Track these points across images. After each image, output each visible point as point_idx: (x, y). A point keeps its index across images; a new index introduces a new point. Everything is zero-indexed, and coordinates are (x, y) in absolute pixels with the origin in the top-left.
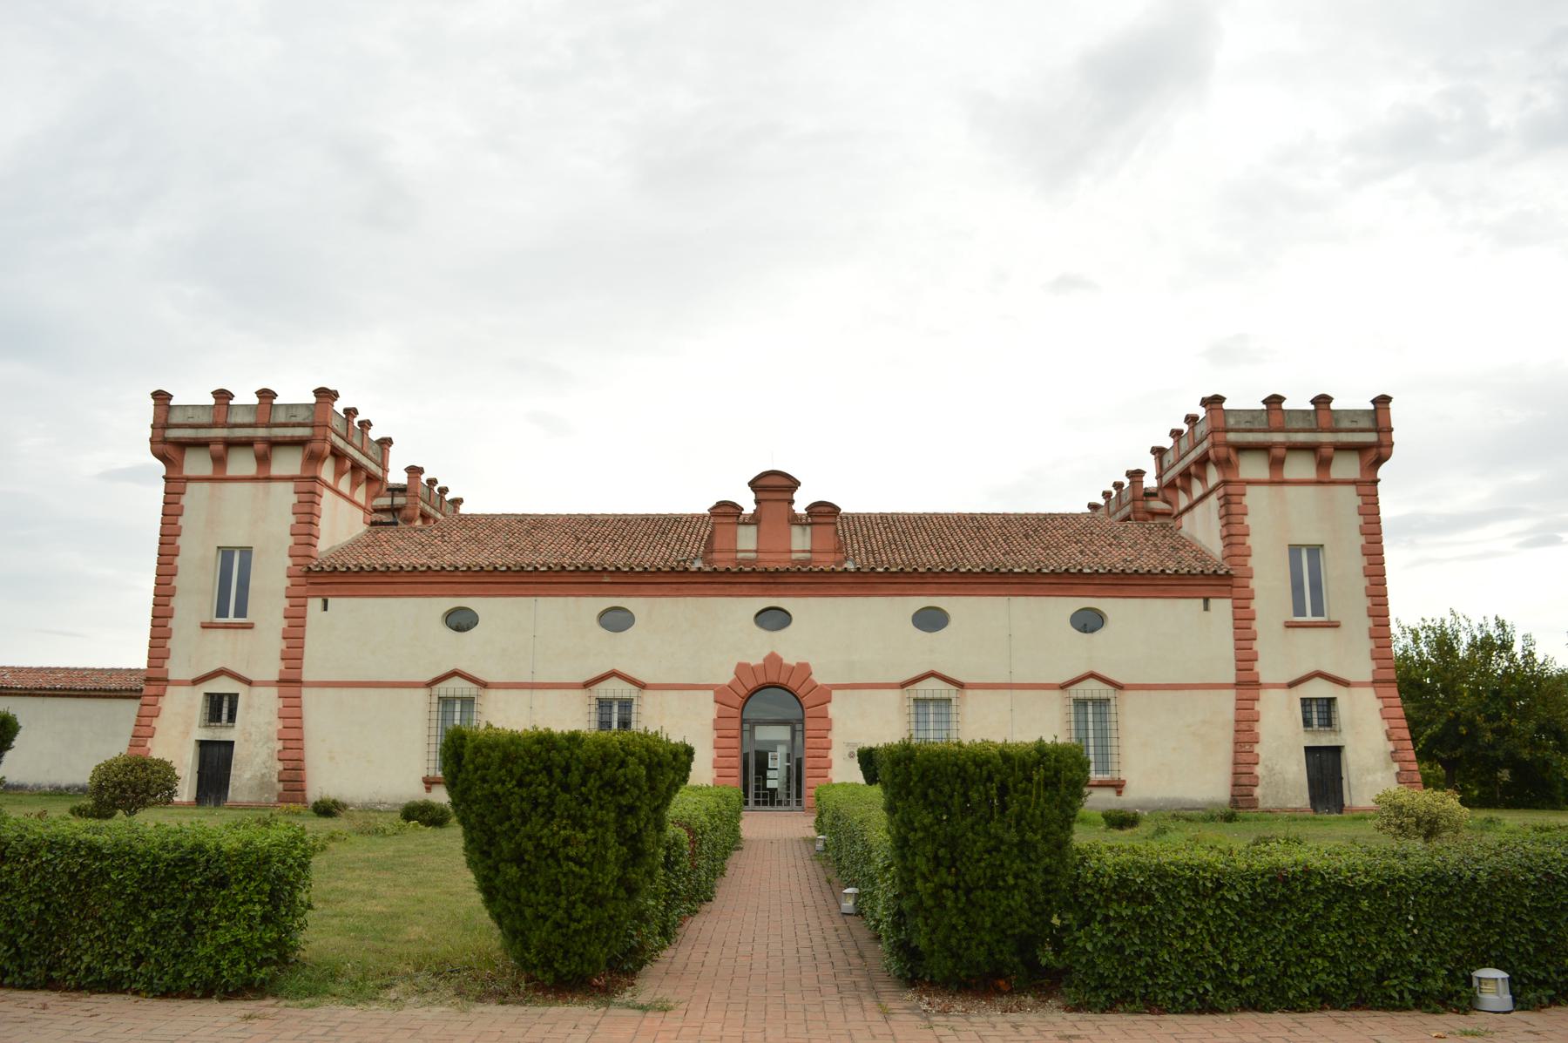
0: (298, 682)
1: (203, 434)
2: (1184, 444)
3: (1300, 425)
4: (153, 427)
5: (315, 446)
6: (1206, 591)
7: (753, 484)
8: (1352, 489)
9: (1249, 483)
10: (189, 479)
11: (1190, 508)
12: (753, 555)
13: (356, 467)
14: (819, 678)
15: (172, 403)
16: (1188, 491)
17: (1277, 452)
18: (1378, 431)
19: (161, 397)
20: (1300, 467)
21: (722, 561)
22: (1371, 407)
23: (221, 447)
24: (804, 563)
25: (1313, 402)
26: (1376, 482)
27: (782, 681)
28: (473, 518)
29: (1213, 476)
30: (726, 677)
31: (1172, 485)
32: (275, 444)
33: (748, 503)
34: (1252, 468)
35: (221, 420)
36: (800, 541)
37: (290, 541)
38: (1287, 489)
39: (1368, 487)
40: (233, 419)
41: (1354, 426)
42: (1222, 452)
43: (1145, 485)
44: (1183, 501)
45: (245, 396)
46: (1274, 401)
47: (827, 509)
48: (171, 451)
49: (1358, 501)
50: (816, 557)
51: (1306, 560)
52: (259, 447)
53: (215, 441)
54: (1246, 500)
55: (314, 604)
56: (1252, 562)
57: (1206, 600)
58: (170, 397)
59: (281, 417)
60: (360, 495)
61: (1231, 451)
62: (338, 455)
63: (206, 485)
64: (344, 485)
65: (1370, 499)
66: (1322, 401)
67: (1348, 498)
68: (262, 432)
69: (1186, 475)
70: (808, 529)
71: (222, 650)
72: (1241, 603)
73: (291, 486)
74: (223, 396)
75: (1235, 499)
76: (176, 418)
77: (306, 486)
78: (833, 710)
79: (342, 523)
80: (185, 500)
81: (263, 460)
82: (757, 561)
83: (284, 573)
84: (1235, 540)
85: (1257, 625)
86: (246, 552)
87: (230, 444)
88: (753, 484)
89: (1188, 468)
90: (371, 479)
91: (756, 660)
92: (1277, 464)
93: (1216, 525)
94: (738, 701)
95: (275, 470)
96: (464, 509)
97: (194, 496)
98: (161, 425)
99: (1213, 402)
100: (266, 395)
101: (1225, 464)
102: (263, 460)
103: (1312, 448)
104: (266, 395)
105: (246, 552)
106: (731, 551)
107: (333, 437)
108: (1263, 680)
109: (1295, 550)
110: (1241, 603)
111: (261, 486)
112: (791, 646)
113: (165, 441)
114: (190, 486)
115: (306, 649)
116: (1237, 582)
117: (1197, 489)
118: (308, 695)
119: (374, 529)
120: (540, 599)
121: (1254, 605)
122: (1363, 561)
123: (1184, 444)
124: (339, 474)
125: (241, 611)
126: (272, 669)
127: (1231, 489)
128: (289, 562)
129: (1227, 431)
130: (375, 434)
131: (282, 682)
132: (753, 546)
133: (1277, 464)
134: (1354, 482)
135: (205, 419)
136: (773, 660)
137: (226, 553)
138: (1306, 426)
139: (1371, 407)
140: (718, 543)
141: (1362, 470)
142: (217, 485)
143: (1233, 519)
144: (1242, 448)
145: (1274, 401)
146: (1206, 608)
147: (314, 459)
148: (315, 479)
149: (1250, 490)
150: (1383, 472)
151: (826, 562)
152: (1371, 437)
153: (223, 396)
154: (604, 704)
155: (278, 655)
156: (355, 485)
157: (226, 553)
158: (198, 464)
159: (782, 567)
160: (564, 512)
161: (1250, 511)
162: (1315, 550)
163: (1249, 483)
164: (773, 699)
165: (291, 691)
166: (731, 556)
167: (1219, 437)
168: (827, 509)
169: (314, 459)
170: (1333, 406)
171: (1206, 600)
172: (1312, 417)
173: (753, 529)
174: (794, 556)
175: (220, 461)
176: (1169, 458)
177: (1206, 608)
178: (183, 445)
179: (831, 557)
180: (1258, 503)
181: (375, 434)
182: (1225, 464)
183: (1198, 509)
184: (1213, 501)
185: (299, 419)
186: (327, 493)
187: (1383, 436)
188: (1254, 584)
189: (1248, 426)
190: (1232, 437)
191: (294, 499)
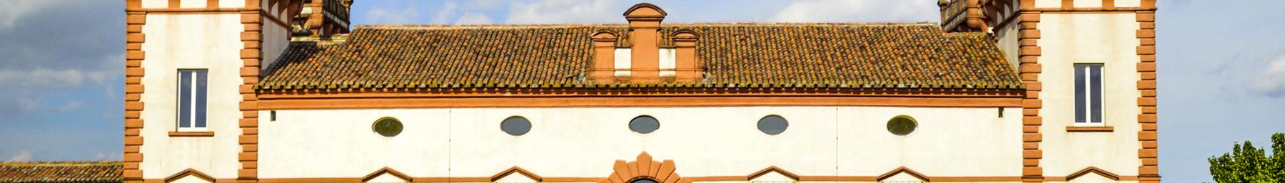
6: (1001, 102)
10: (147, 12)
21: (602, 78)
24: (668, 79)
27: (652, 174)
36: (667, 61)
38: (1075, 16)
49: (1138, 26)
50: (680, 74)
55: (264, 116)
57: (1001, 109)
63: (164, 16)
70: (673, 51)
71: (187, 153)
72: (1030, 111)
73: (238, 16)
75: (1030, 25)
82: (630, 78)
83: (237, 90)
86: (202, 73)
91: (631, 158)
105: (202, 73)
106: (609, 70)
108: (1044, 175)
109: (1079, 67)
110: (1030, 111)
111: (212, 16)
112: (657, 147)
115: (259, 152)
120: (453, 110)
121: (1041, 113)
125: (201, 121)
128: (241, 81)
136: (644, 158)
137: (185, 74)
143: (1026, 42)
146: (1001, 115)
149: (1042, 15)
151: (689, 78)
155: (237, 159)
156: (280, 11)
157: (185, 74)
159: (652, 83)
162: (1096, 68)
166: (610, 74)
171: (1001, 109)
174: (662, 74)
177: (1001, 115)
188: (1041, 95)
191: (242, 28)
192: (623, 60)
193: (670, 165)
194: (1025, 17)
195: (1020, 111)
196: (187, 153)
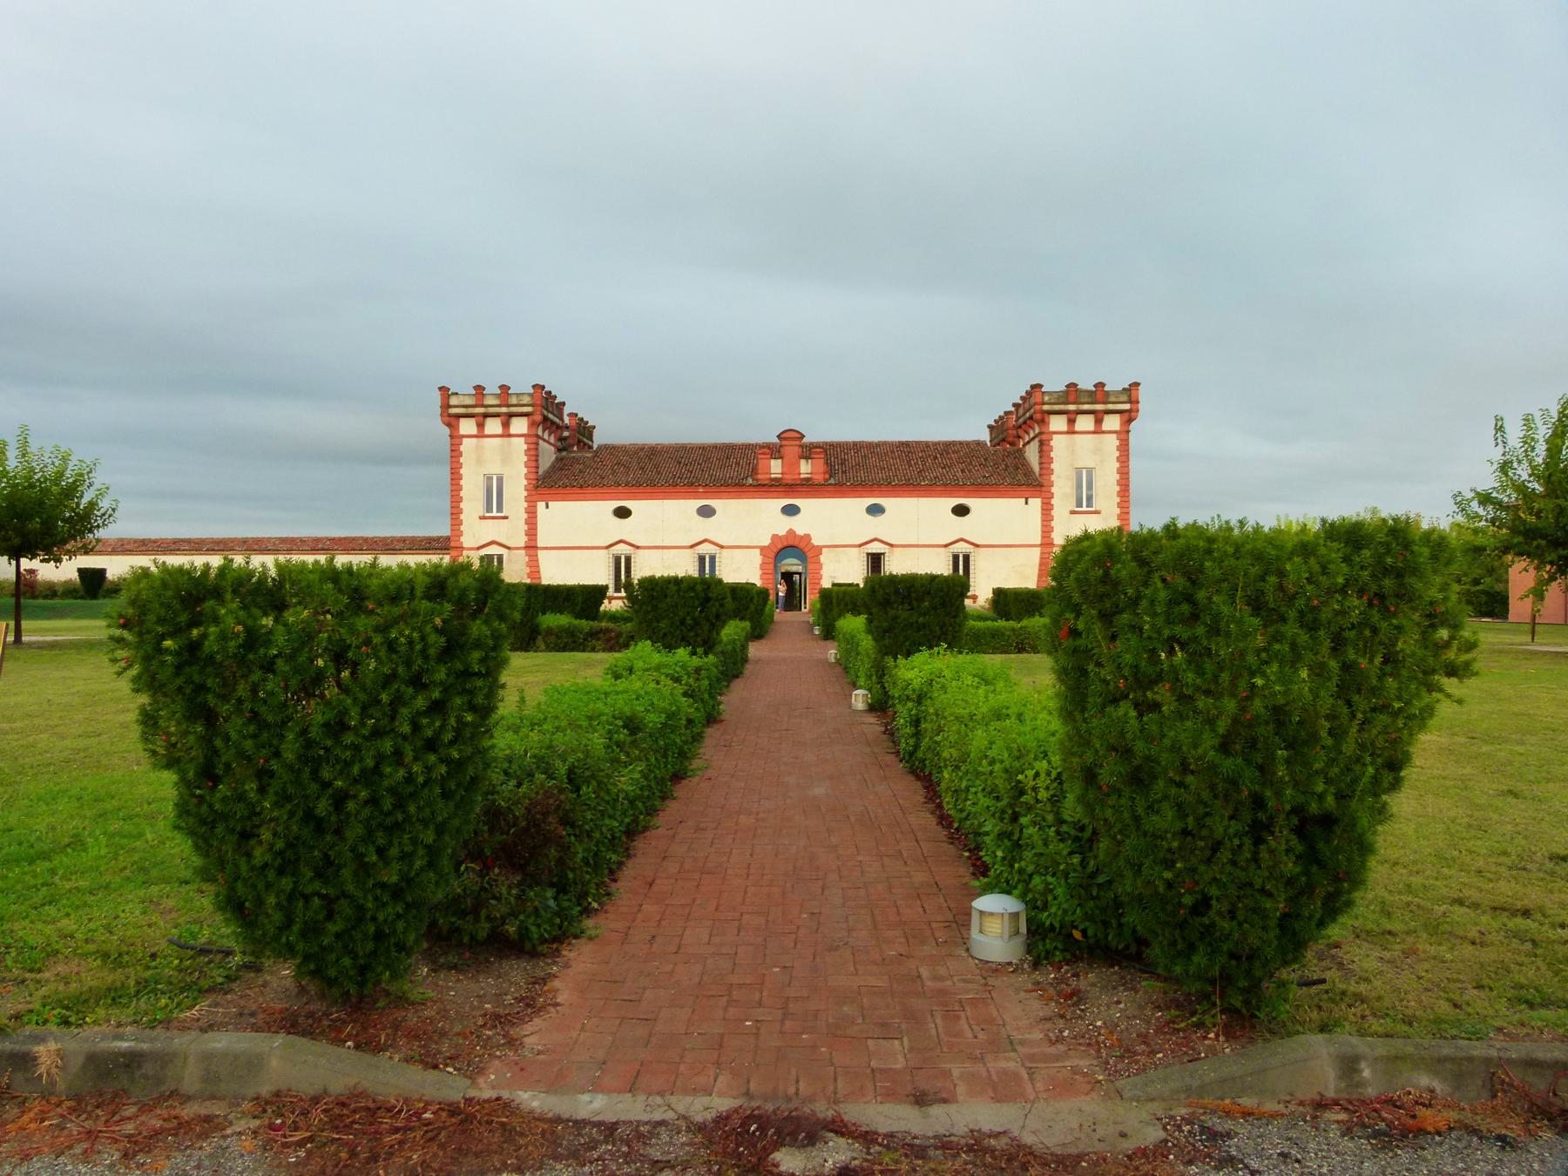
0: (536, 548)
1: (471, 410)
2: (1021, 411)
14: (816, 542)
18: (1130, 402)
19: (443, 389)
20: (1086, 423)
24: (807, 480)
30: (766, 542)
36: (805, 468)
39: (1124, 435)
55: (541, 505)
56: (1053, 478)
66: (1100, 385)
67: (1112, 442)
68: (504, 410)
71: (491, 531)
76: (453, 401)
78: (822, 558)
85: (1054, 513)
87: (486, 416)
91: (782, 532)
94: (772, 555)
95: (513, 431)
98: (446, 406)
100: (505, 388)
109: (1079, 471)
112: (799, 525)
113: (450, 415)
114: (465, 440)
118: (540, 553)
123: (1021, 411)
125: (500, 509)
126: (521, 540)
131: (527, 548)
136: (791, 532)
151: (819, 478)
152: (1127, 407)
154: (702, 559)
162: (1090, 471)
164: (790, 551)
165: (532, 552)
180: (1059, 444)
188: (1053, 490)
190: (1046, 407)
192: (776, 467)
193: (808, 537)
194: (1044, 437)
195: (1038, 501)
196: (491, 531)
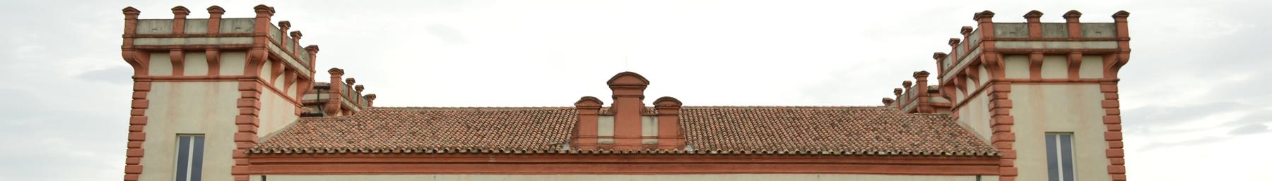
1: (165, 42)
2: (961, 51)
3: (1055, 35)
4: (124, 37)
5: (256, 52)
7: (611, 83)
8: (1097, 87)
9: (1014, 82)
10: (153, 79)
11: (965, 102)
12: (611, 141)
13: (289, 70)
15: (140, 17)
16: (963, 89)
17: (1036, 57)
18: (1118, 40)
19: (131, 13)
20: (1055, 69)
21: (585, 145)
22: (1113, 21)
23: (179, 53)
25: (1065, 16)
26: (1116, 81)
28: (384, 110)
29: (984, 77)
31: (950, 84)
32: (223, 50)
33: (607, 99)
34: (1016, 70)
35: (179, 31)
36: (649, 129)
37: (235, 129)
39: (1110, 85)
40: (190, 30)
41: (1098, 36)
42: (991, 57)
43: (929, 84)
44: (960, 97)
45: (199, 12)
46: (1034, 16)
47: (671, 103)
48: (139, 57)
49: (1102, 97)
50: (662, 141)
51: (1059, 145)
52: (210, 53)
53: (174, 48)
54: (1011, 96)
58: (138, 12)
59: (228, 29)
60: (292, 92)
61: (999, 57)
62: (274, 60)
63: (167, 84)
64: (279, 83)
65: (1111, 96)
66: (1073, 16)
67: (1094, 94)
68: (212, 41)
69: (962, 76)
70: (656, 119)
73: (236, 84)
74: (181, 12)
75: (1002, 95)
76: (143, 29)
77: (249, 85)
79: (277, 114)
80: (150, 96)
81: (214, 64)
82: (614, 145)
84: (1002, 128)
87: (187, 50)
88: (611, 83)
89: (964, 70)
90: (301, 79)
92: (1036, 67)
93: (987, 116)
95: (224, 72)
96: (376, 103)
97: (158, 92)
99: (984, 17)
100: (216, 11)
101: (994, 67)
102: (214, 64)
103: (1064, 54)
104: (216, 11)
107: (270, 45)
111: (212, 84)
113: (134, 48)
114: (154, 85)
116: (1003, 162)
117: (971, 87)
119: (303, 119)
122: (1106, 146)
123: (961, 51)
124: (275, 75)
127: (999, 87)
129: (996, 40)
130: (304, 43)
132: (611, 133)
133: (1036, 67)
134: (1098, 82)
135: (167, 30)
138: (1060, 36)
139: (1113, 21)
140: (583, 131)
141: (1105, 72)
142: (176, 84)
144: (1007, 54)
145: (1034, 16)
147: (255, 62)
148: (256, 79)
149: (1014, 87)
150: (1122, 73)
151: (671, 146)
152: (1112, 45)
153: (181, 12)
158: (161, 66)
159: (634, 150)
160: (458, 106)
161: (1014, 105)
163: (1014, 82)
166: (593, 141)
167: (989, 45)
168: (671, 103)
169: (255, 62)
170: (1082, 20)
172: (1064, 29)
173: (611, 119)
174: (644, 141)
175: (178, 64)
176: (949, 62)
178: (149, 52)
179: (674, 142)
180: (1020, 97)
181: (304, 43)
182: (994, 67)
183: (972, 103)
184: (984, 96)
185: (243, 31)
186: (265, 91)
187: (1122, 45)
189: (1013, 36)
190: (999, 45)
191: (238, 95)
